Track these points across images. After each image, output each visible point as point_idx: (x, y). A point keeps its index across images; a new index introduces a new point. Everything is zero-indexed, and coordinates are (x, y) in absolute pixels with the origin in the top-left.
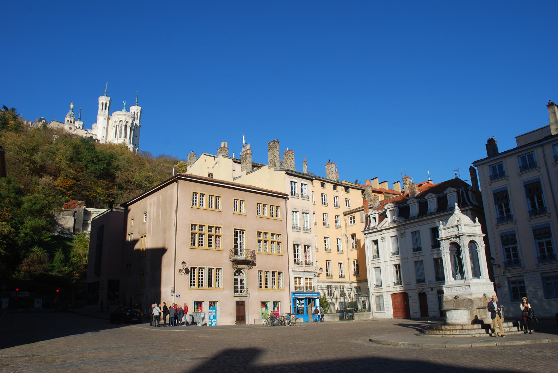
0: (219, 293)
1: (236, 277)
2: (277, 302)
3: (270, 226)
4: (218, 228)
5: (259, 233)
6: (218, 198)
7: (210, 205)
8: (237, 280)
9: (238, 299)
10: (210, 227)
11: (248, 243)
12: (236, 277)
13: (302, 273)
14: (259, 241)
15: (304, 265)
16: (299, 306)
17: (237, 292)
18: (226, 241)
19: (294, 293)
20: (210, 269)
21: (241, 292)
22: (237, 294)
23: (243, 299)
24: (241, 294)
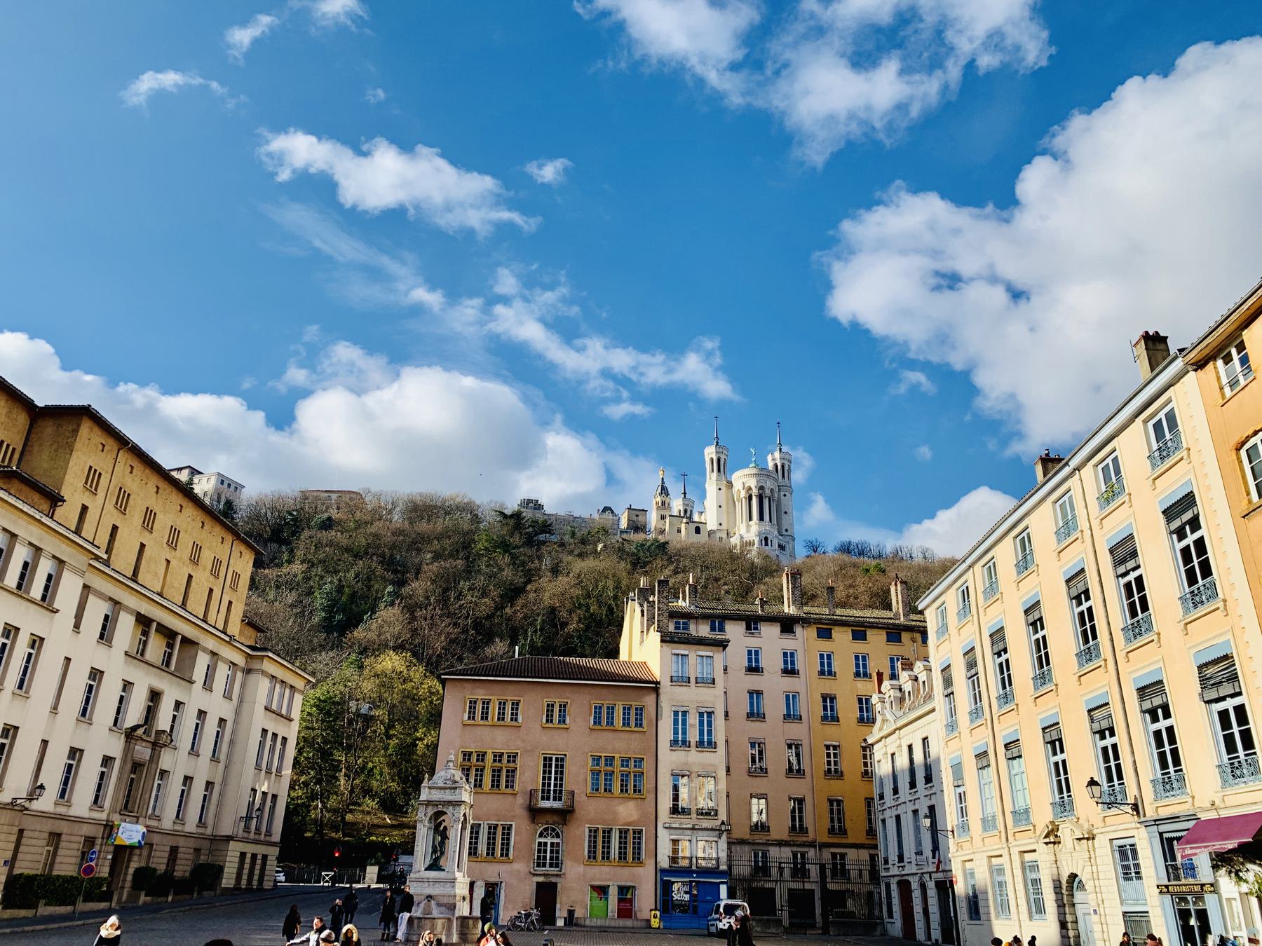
0: (503, 868)
1: (543, 840)
2: (628, 888)
3: (619, 744)
4: (513, 757)
5: (597, 760)
6: (516, 705)
7: (501, 717)
8: (546, 844)
9: (541, 879)
10: (498, 757)
11: (577, 777)
12: (543, 840)
13: (689, 832)
14: (596, 774)
15: (694, 816)
16: (676, 897)
17: (544, 865)
18: (529, 776)
19: (663, 871)
20: (493, 829)
21: (551, 866)
22: (541, 870)
23: (553, 880)
24: (554, 870)
